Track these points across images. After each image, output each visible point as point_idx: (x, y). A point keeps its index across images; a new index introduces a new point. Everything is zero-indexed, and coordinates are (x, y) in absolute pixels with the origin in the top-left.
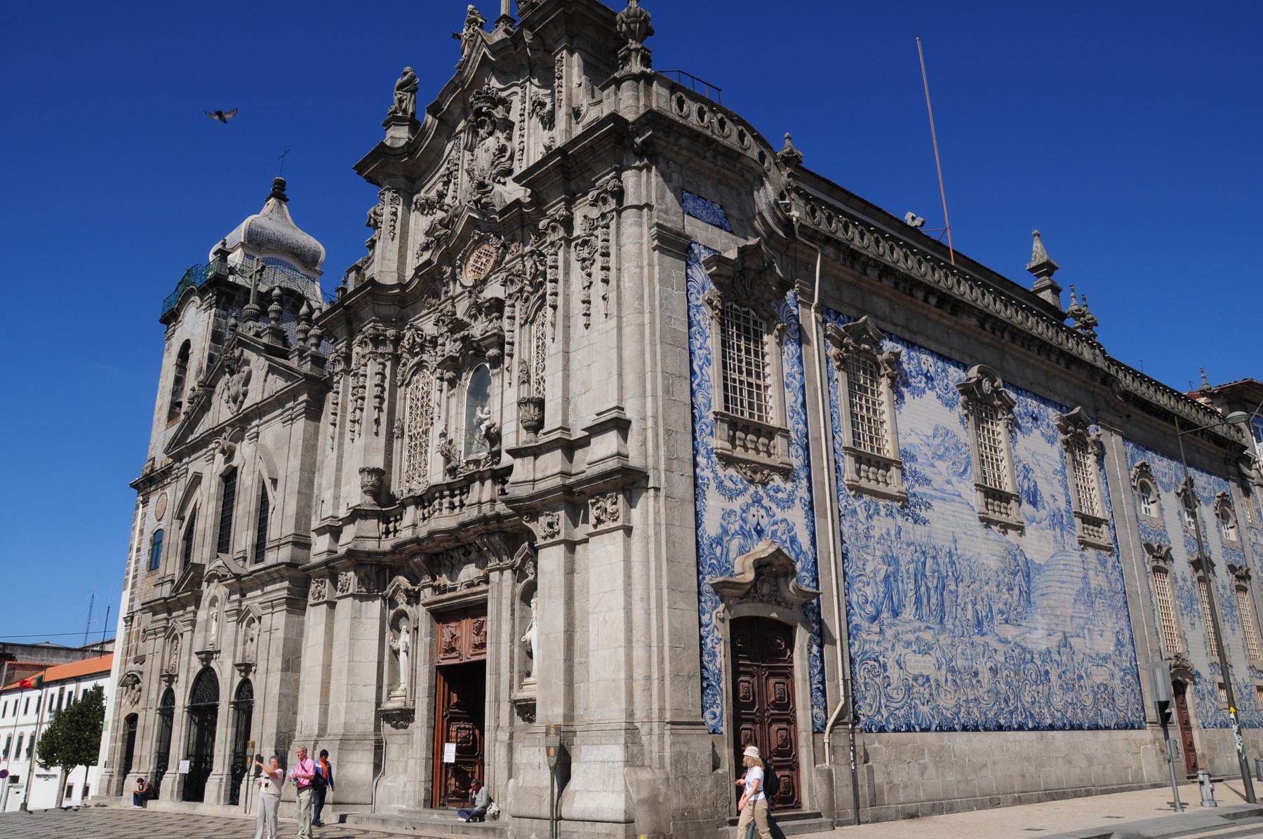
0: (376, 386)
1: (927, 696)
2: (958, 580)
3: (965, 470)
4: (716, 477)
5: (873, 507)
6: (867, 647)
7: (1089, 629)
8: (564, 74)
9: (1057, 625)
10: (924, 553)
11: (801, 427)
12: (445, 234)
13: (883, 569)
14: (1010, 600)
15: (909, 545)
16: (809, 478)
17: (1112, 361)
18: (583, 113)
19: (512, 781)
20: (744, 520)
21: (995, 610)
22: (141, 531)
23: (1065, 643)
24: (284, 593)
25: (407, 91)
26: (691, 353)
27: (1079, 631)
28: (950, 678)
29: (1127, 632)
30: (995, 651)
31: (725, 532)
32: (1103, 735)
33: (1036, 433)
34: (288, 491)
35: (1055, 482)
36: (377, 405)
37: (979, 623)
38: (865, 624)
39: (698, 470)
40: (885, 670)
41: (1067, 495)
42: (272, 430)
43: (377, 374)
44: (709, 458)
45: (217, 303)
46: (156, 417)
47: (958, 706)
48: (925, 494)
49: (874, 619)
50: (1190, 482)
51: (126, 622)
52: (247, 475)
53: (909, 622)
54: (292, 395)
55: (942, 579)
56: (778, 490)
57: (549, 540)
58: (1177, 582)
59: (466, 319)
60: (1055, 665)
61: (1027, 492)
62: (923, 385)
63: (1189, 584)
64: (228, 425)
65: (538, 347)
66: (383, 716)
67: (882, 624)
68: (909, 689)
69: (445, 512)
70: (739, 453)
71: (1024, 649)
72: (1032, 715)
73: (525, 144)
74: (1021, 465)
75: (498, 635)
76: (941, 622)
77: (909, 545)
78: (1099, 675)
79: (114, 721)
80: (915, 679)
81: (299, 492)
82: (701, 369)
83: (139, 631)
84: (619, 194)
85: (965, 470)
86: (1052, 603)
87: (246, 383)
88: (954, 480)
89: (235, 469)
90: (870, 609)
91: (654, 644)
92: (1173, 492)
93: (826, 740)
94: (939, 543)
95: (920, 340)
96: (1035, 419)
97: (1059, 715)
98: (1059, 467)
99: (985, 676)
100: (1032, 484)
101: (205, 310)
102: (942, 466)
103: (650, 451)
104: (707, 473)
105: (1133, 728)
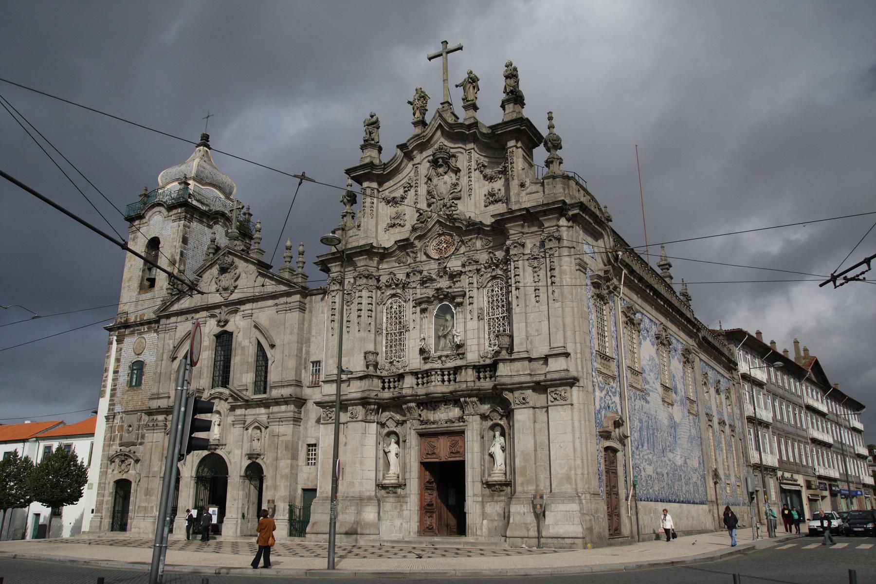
0: (369, 304)
4: (598, 382)
8: (515, 161)
10: (649, 417)
11: (617, 357)
12: (421, 227)
15: (645, 413)
16: (620, 381)
17: (695, 319)
18: (527, 186)
19: (485, 522)
22: (118, 360)
23: (685, 462)
24: (291, 414)
25: (373, 127)
32: (696, 505)
34: (286, 353)
35: (682, 384)
36: (370, 315)
38: (635, 451)
40: (640, 470)
42: (265, 313)
43: (369, 297)
45: (185, 218)
46: (125, 284)
47: (659, 490)
50: (719, 381)
51: (107, 418)
52: (244, 338)
53: (646, 450)
54: (288, 294)
55: (653, 430)
56: (612, 388)
57: (524, 406)
59: (434, 277)
62: (646, 335)
64: (222, 305)
65: (489, 302)
66: (381, 486)
68: (647, 482)
69: (440, 383)
70: (603, 370)
71: (675, 464)
73: (473, 186)
75: (473, 448)
76: (654, 451)
79: (100, 483)
81: (297, 356)
83: (122, 427)
84: (559, 239)
86: (682, 442)
87: (236, 281)
88: (655, 381)
89: (231, 334)
90: (636, 444)
91: (585, 458)
93: (629, 504)
94: (652, 413)
95: (645, 312)
96: (675, 351)
97: (684, 496)
98: (682, 374)
99: (665, 476)
101: (174, 221)
102: (652, 374)
103: (580, 369)
104: (595, 380)
105: (704, 504)
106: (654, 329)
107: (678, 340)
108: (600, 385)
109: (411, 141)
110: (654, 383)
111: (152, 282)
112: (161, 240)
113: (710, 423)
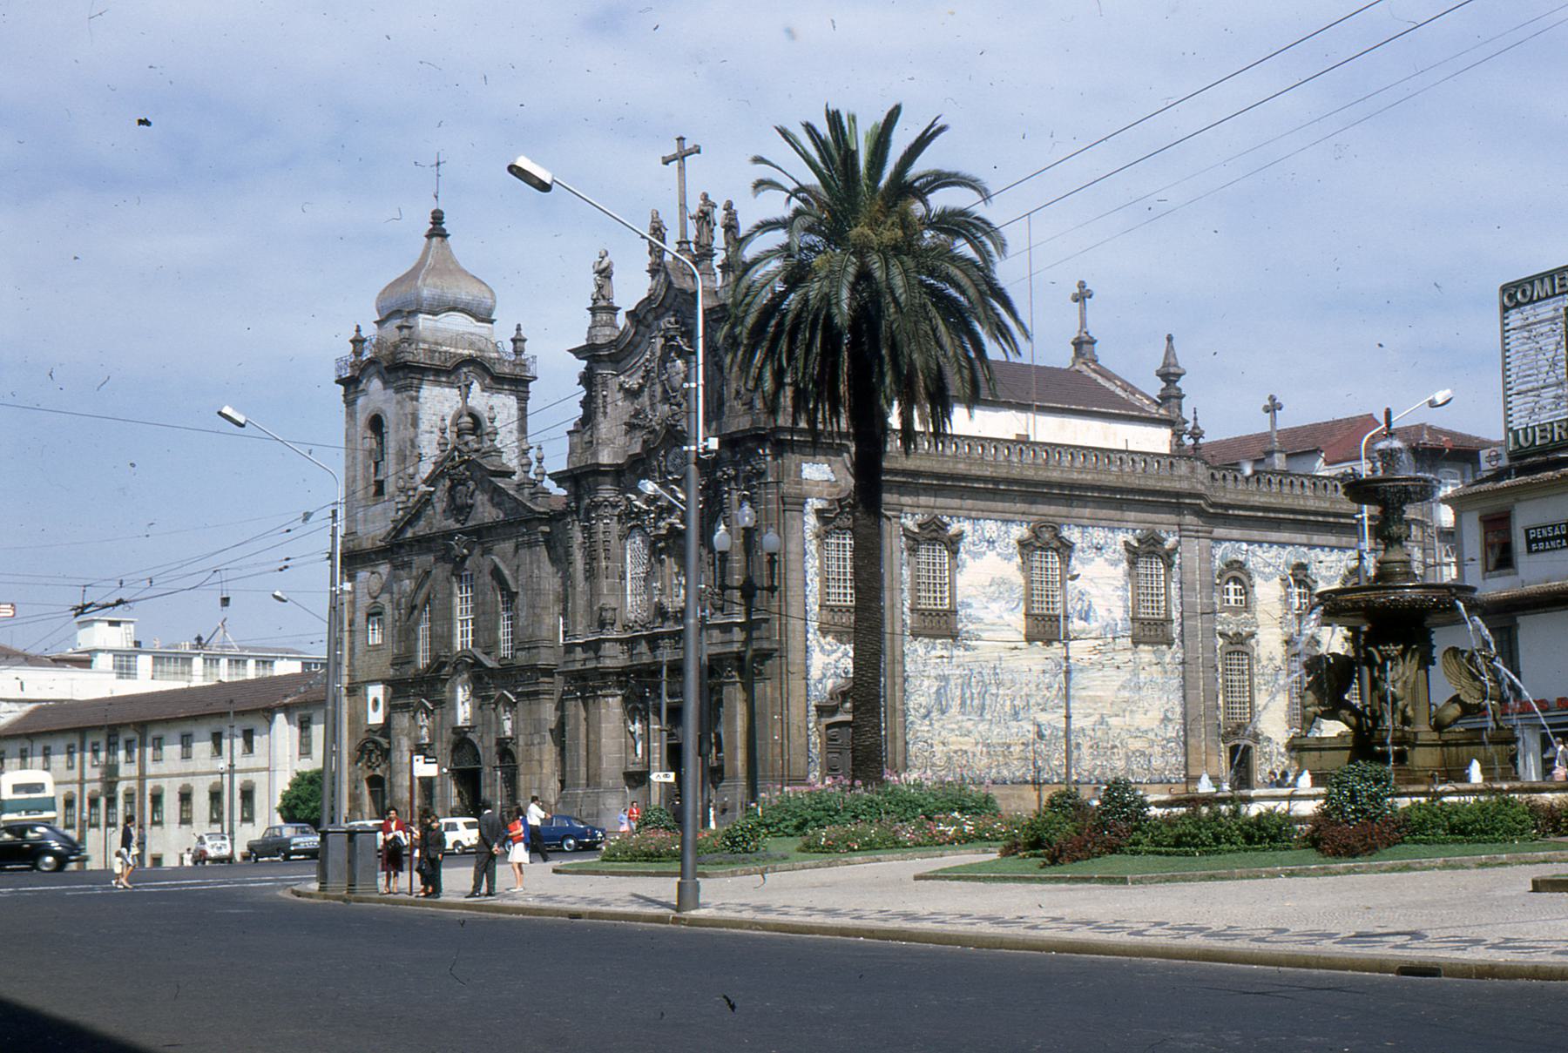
1: (964, 762)
2: (999, 685)
3: (1018, 605)
4: (818, 642)
5: (931, 645)
6: (919, 734)
7: (1131, 711)
9: (1095, 709)
10: (970, 670)
13: (936, 684)
14: (1048, 694)
20: (837, 668)
21: (1032, 702)
23: (1102, 721)
26: (806, 572)
27: (1121, 714)
28: (984, 749)
29: (1178, 710)
30: (1029, 731)
31: (824, 675)
33: (1099, 561)
37: (1016, 713)
39: (808, 643)
40: (932, 747)
41: (1126, 606)
44: (815, 634)
48: (977, 630)
49: (925, 717)
50: (1302, 567)
53: (954, 716)
58: (1259, 661)
60: (1088, 739)
61: (1080, 611)
63: (1278, 662)
67: (931, 720)
72: (1058, 774)
74: (1076, 591)
76: (981, 715)
77: (958, 667)
78: (1138, 744)
80: (956, 752)
82: (812, 580)
85: (1018, 605)
86: (1090, 693)
90: (923, 711)
92: (1277, 580)
97: (1086, 773)
100: (1086, 603)
102: (994, 606)
106: (1019, 531)
107: (1112, 529)
108: (827, 647)
109: (640, 307)
110: (1000, 617)
111: (380, 488)
112: (384, 418)
113: (1239, 647)
